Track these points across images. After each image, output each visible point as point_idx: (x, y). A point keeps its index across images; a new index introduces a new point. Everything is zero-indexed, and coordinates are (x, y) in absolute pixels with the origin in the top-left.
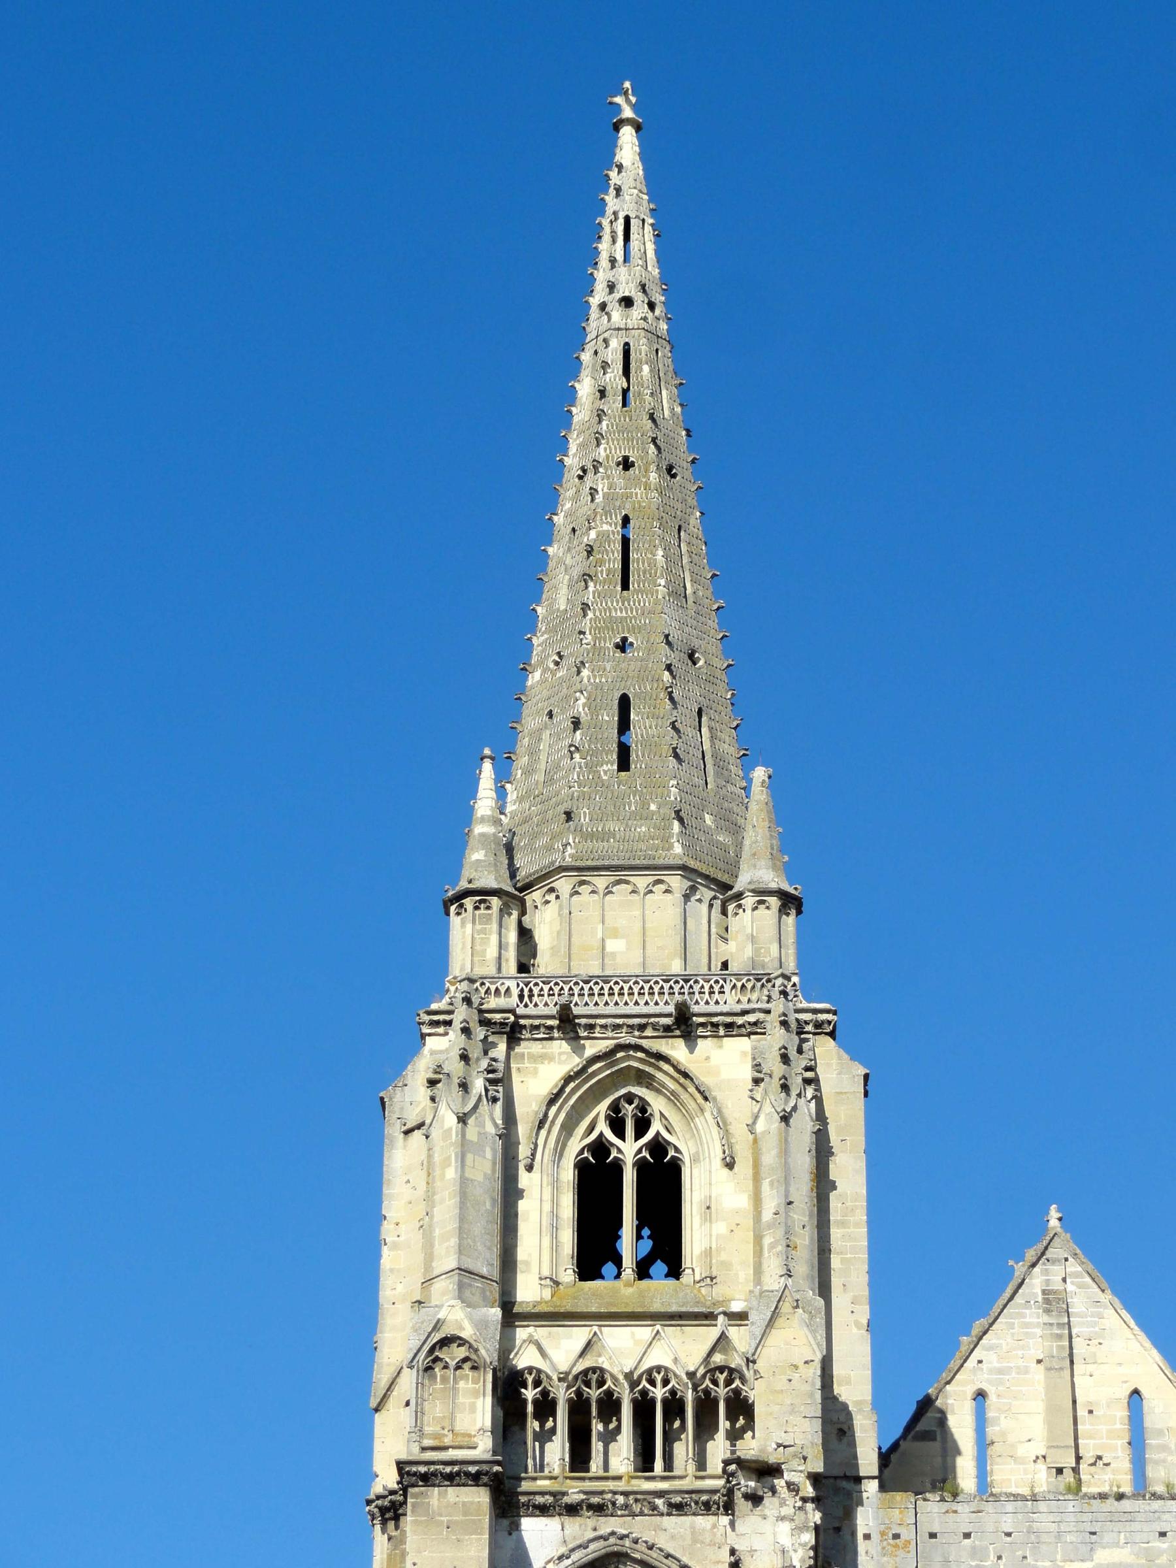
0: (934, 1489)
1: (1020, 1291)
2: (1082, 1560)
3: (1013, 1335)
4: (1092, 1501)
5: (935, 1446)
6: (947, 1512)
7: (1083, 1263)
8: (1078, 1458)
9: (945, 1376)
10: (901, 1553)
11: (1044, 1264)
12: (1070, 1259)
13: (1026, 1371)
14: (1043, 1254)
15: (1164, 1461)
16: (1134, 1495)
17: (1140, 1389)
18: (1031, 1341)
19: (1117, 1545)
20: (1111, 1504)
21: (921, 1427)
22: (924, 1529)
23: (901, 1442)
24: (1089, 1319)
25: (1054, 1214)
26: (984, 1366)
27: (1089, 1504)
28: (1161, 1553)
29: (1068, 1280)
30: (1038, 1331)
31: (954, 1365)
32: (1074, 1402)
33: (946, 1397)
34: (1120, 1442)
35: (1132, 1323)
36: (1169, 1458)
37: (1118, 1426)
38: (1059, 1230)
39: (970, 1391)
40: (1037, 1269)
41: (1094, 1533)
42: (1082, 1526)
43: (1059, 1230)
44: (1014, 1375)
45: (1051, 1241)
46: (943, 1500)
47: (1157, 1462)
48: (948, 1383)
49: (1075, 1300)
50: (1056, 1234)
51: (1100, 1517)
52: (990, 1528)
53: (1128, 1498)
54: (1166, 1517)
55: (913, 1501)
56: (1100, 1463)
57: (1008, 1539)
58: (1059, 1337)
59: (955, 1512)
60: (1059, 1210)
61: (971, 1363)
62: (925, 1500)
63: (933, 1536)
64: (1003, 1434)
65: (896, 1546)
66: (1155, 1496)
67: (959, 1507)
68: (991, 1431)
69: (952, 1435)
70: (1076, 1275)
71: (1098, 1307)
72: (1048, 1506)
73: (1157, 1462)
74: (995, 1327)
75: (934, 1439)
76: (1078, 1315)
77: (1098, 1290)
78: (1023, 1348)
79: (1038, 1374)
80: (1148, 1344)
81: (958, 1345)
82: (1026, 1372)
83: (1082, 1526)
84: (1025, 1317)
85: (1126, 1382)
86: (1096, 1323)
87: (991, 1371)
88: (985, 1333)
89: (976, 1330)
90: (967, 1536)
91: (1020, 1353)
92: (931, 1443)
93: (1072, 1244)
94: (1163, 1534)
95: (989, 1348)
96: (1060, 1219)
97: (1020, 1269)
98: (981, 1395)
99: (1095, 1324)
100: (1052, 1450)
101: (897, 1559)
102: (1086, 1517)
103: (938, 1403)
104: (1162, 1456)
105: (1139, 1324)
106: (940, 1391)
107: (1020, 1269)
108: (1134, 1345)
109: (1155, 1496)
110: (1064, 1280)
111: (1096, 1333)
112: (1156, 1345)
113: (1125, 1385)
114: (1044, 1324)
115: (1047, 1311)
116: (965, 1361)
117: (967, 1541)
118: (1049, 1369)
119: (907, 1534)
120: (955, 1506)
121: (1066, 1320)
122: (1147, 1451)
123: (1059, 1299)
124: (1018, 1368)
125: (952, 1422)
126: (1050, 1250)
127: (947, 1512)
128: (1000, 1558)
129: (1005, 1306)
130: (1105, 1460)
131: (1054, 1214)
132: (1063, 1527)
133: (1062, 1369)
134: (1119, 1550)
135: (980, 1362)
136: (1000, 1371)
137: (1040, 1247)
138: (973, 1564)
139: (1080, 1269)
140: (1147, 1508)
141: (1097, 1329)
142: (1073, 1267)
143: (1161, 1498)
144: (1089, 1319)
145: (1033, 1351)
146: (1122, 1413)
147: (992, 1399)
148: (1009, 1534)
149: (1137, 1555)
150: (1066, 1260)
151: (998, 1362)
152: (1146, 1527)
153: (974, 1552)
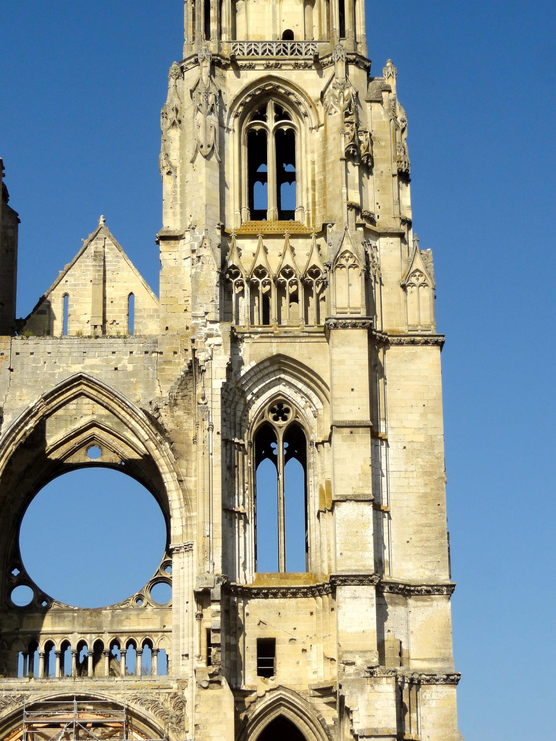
0: (19, 334)
1: (85, 252)
2: (79, 364)
3: (81, 270)
4: (85, 339)
5: (45, 317)
6: (24, 344)
7: (112, 240)
8: (105, 321)
9: (52, 287)
10: (4, 361)
11: (96, 240)
12: (107, 238)
13: (86, 285)
14: (96, 236)
15: (142, 322)
16: (103, 337)
17: (133, 292)
18: (88, 273)
19: (94, 357)
20: (93, 340)
21: (40, 308)
22: (14, 351)
23: (31, 315)
24: (114, 263)
25: (102, 219)
26: (68, 283)
27: (84, 340)
28: (112, 360)
29: (106, 247)
30: (91, 268)
31: (56, 283)
32: (105, 298)
33: (51, 296)
34: (123, 315)
35: (132, 265)
36: (144, 321)
37: (123, 308)
38: (103, 226)
39: (62, 293)
40: (93, 243)
41: (85, 352)
42: (80, 349)
43: (103, 226)
44: (80, 287)
45: (99, 230)
46: (22, 339)
47: (138, 323)
48: (53, 290)
49: (108, 255)
50: (101, 228)
51: (88, 345)
52: (41, 350)
53: (100, 338)
54: (115, 345)
55: (10, 339)
56: (115, 323)
57: (49, 355)
58: (99, 271)
59: (28, 344)
60: (104, 218)
61: (63, 282)
62: (15, 339)
63: (17, 354)
64: (75, 311)
65: (2, 358)
66: (111, 337)
67: (29, 342)
68: (70, 310)
69: (53, 311)
70: (109, 245)
71: (118, 258)
72: (67, 341)
73: (138, 323)
74: (73, 267)
75: (45, 314)
76: (109, 261)
77: (118, 251)
78: (85, 275)
79: (90, 286)
80: (138, 274)
81: (58, 274)
82: (86, 286)
83: (80, 349)
84: (87, 263)
85: (128, 289)
86: (116, 265)
87: (71, 285)
88: (69, 269)
89: (66, 268)
90: (32, 354)
91: (84, 278)
92: (44, 315)
93: (108, 232)
94: (114, 353)
95: (71, 276)
96: (104, 221)
97: (86, 242)
98: (66, 295)
99: (116, 265)
100: (93, 318)
101: (2, 363)
102: (82, 346)
103: (48, 298)
104: (141, 320)
105: (134, 265)
106: (49, 294)
107: (86, 242)
108: (132, 274)
109: (111, 337)
110: (104, 247)
111: (116, 269)
112: (142, 273)
113: (127, 291)
114: (93, 265)
115: (95, 260)
116: (60, 281)
117: (32, 356)
118: (93, 284)
119: (7, 353)
120: (27, 341)
121: (102, 264)
122: (135, 318)
123: (101, 255)
124: (82, 284)
125: (53, 306)
126: (99, 234)
127: (24, 344)
128: (45, 363)
129: (78, 258)
130: (117, 322)
131: (102, 219)
132: (72, 350)
133: (99, 284)
134: (95, 359)
135: (66, 281)
136: (75, 285)
137: (95, 233)
138: (34, 365)
139: (111, 242)
140: (108, 342)
141: (117, 268)
142: (108, 241)
143: (114, 337)
144: (114, 263)
145: (89, 277)
146: (125, 302)
147: (71, 296)
148: (49, 353)
149: (102, 361)
150: (105, 238)
151: (74, 281)
152: (107, 350)
153: (34, 361)
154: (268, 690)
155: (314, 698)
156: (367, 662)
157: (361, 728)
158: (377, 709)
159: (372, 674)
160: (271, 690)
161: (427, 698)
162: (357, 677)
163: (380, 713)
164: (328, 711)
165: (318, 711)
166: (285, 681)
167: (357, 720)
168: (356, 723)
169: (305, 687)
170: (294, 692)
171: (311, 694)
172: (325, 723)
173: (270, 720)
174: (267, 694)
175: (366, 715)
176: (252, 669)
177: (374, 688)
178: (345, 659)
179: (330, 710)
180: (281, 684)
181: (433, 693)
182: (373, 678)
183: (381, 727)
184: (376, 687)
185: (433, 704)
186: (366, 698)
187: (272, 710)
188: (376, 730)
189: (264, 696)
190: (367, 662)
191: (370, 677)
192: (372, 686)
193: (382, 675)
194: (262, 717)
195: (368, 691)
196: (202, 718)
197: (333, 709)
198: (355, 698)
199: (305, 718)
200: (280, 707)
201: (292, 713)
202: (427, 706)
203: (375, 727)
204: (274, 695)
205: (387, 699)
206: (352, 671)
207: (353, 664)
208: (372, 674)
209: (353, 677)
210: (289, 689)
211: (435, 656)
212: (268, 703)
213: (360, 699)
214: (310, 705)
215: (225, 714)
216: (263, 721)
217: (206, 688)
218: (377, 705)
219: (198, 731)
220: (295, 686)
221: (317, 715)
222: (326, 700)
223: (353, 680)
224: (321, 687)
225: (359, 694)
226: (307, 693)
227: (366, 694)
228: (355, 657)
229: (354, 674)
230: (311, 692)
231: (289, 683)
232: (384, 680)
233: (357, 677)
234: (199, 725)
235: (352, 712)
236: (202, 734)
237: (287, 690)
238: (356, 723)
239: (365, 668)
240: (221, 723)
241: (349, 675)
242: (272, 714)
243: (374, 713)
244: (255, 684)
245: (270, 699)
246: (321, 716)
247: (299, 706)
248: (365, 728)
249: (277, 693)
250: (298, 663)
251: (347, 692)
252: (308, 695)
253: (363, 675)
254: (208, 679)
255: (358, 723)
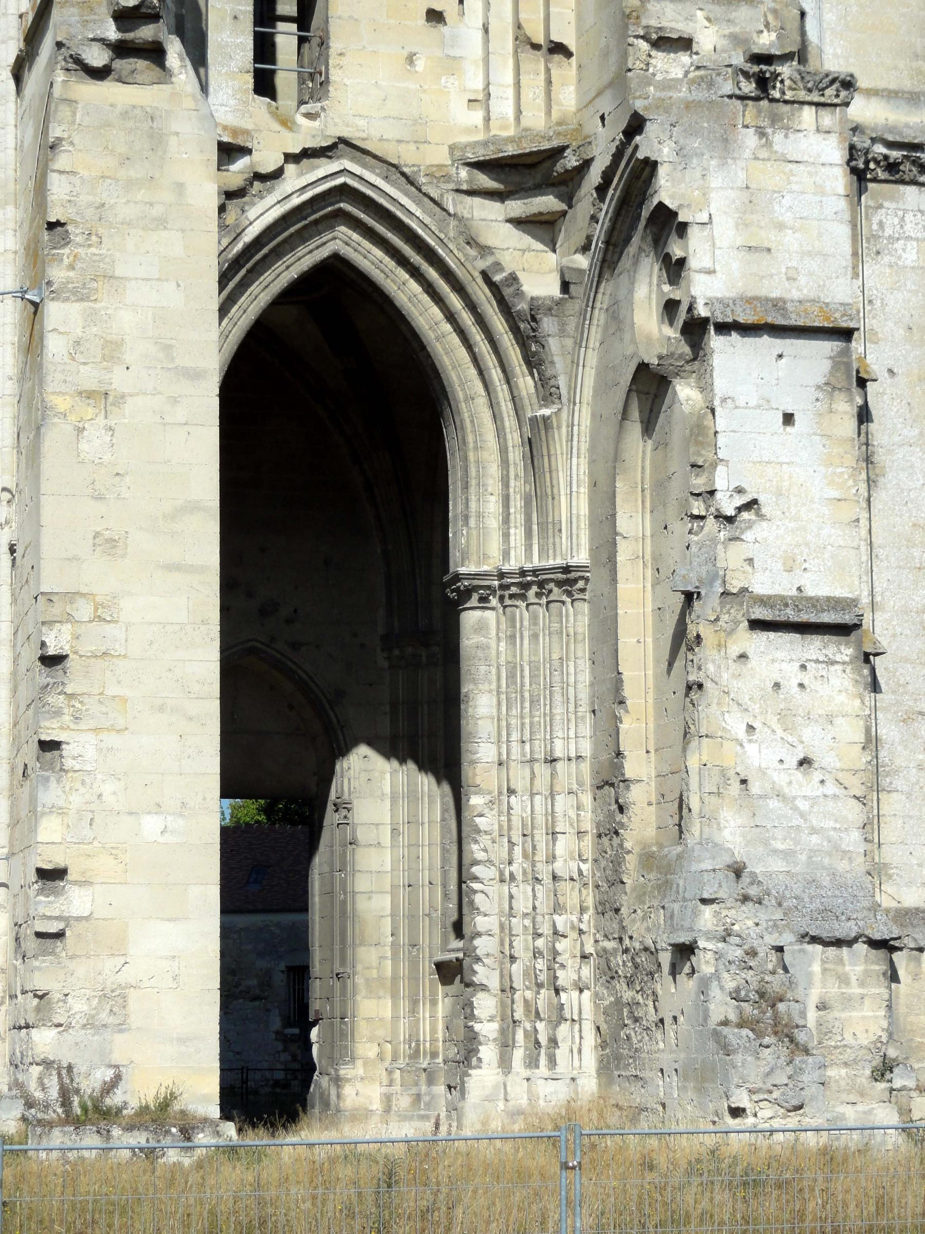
154: (297, 150)
155: (468, 200)
156: (737, 40)
157: (719, 295)
158: (781, 226)
159: (763, 83)
160: (307, 154)
161: (888, 232)
162: (700, 95)
163: (790, 240)
164: (524, 251)
165: (485, 250)
166: (361, 123)
167: (707, 263)
168: (700, 271)
169: (439, 156)
170: (393, 169)
171: (459, 182)
172: (519, 293)
173: (293, 273)
174: (290, 168)
175: (738, 244)
176: (234, 66)
177: (769, 144)
178: (653, 23)
179: (529, 250)
180: (346, 133)
181: (909, 217)
182: (764, 103)
183: (795, 294)
184: (778, 138)
185: (910, 255)
186: (741, 178)
187: (302, 237)
188: (778, 304)
189: (277, 174)
190: (737, 40)
191: (757, 99)
192: (761, 133)
193: (802, 95)
194: (265, 257)
195: (747, 154)
196: (84, 199)
197: (539, 246)
198: (698, 174)
199: (432, 274)
200: (332, 228)
201: (378, 253)
202: (887, 259)
203: (774, 295)
204: (321, 173)
205: (820, 190)
206: (677, 73)
207: (685, 44)
208: (763, 83)
209: (683, 93)
210: (375, 157)
211: (908, 84)
212: (296, 201)
213: (716, 181)
214: (453, 223)
215: (180, 187)
216: (268, 276)
217: (99, 74)
218: (782, 211)
219: (66, 251)
220: (402, 148)
221: (482, 264)
222: (517, 207)
223: (689, 106)
224: (511, 150)
225: (713, 162)
226: (447, 178)
227: (741, 164)
228: (691, 18)
229: (692, 82)
230: (464, 173)
231: (375, 133)
232: (808, 113)
233: (700, 95)
234: (70, 228)
235: (682, 228)
236: (79, 265)
237: (368, 159)
238: (700, 271)
239: (739, 59)
240: (161, 223)
241: (669, 85)
242: (301, 250)
243: (768, 237)
244: (247, 124)
245: (303, 189)
246: (498, 266)
247: (414, 225)
248: (732, 294)
249: (326, 167)
250: (410, 59)
251: (666, 150)
252: (452, 186)
253: (728, 88)
254: (112, 33)
255: (711, 272)
